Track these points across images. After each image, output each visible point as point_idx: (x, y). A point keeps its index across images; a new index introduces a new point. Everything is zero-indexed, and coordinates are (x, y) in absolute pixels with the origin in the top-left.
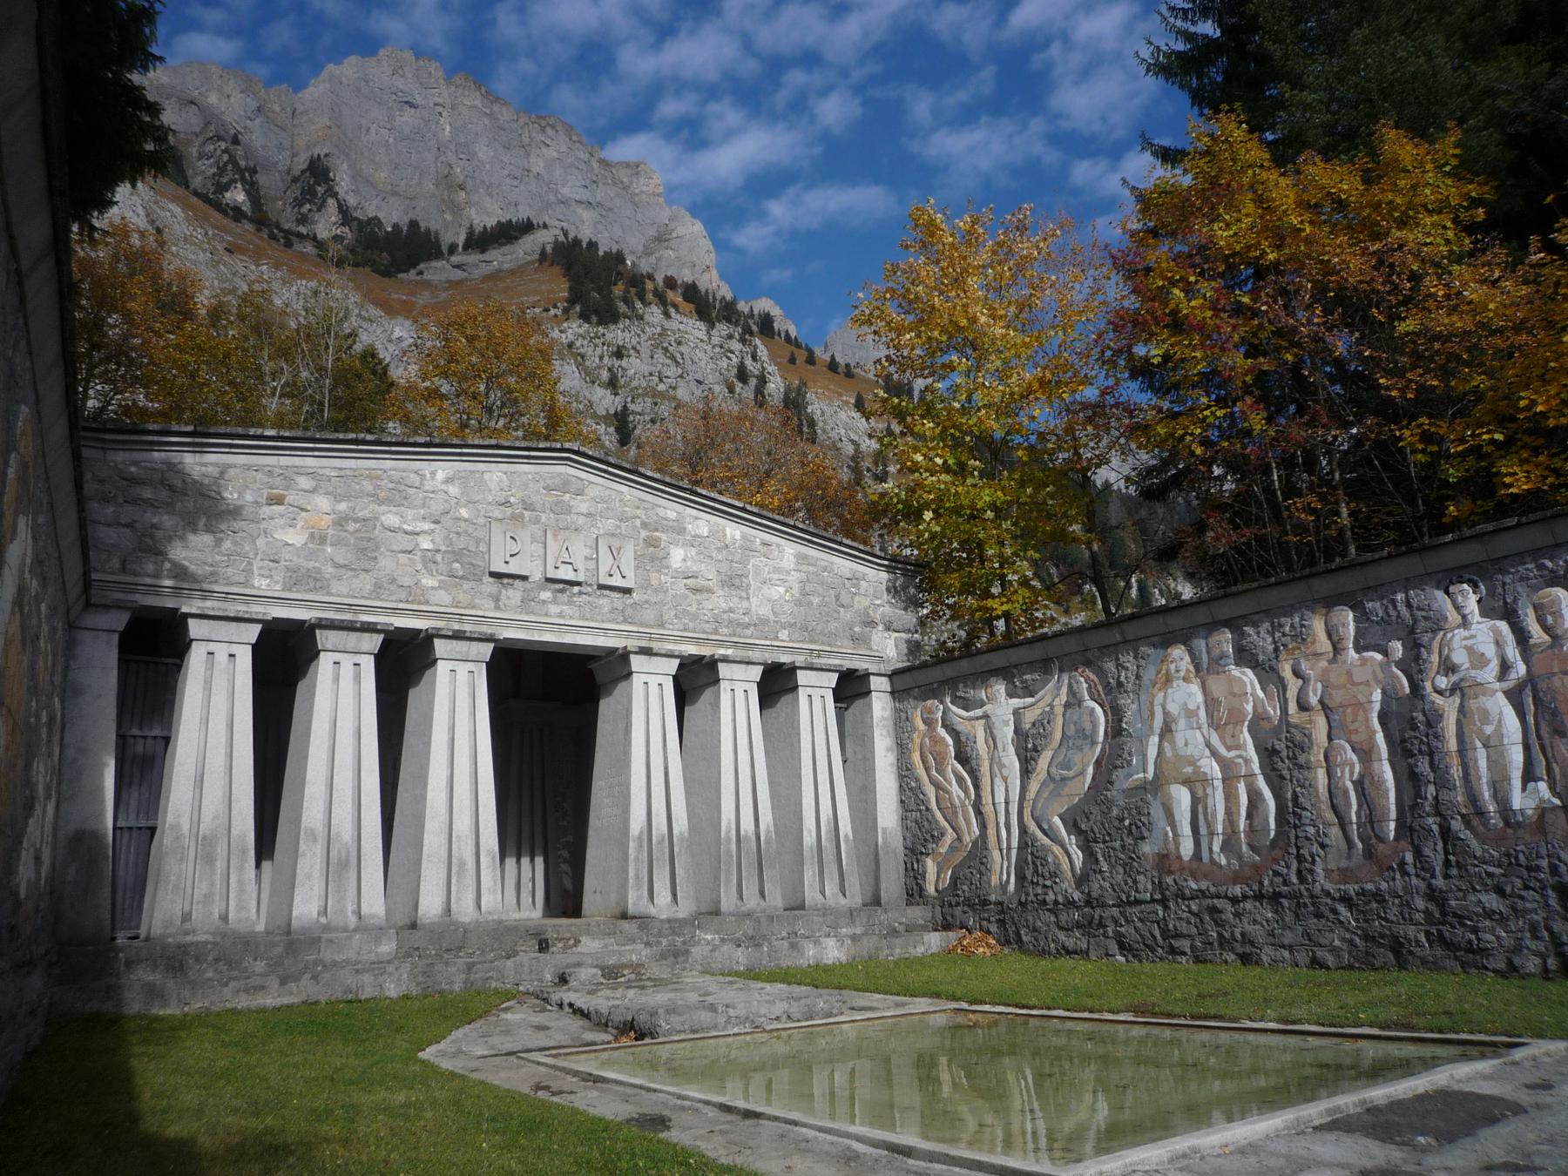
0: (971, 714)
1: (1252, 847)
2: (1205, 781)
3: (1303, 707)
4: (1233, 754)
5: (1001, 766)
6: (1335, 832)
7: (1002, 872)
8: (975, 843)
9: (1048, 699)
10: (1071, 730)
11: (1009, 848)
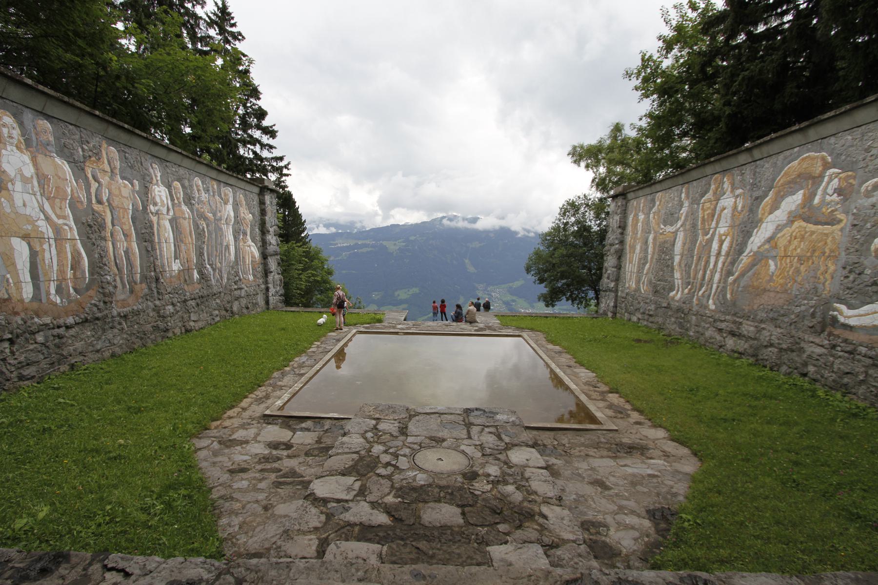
1: (75, 290)
2: (41, 238)
3: (100, 202)
4: (61, 222)
6: (118, 279)
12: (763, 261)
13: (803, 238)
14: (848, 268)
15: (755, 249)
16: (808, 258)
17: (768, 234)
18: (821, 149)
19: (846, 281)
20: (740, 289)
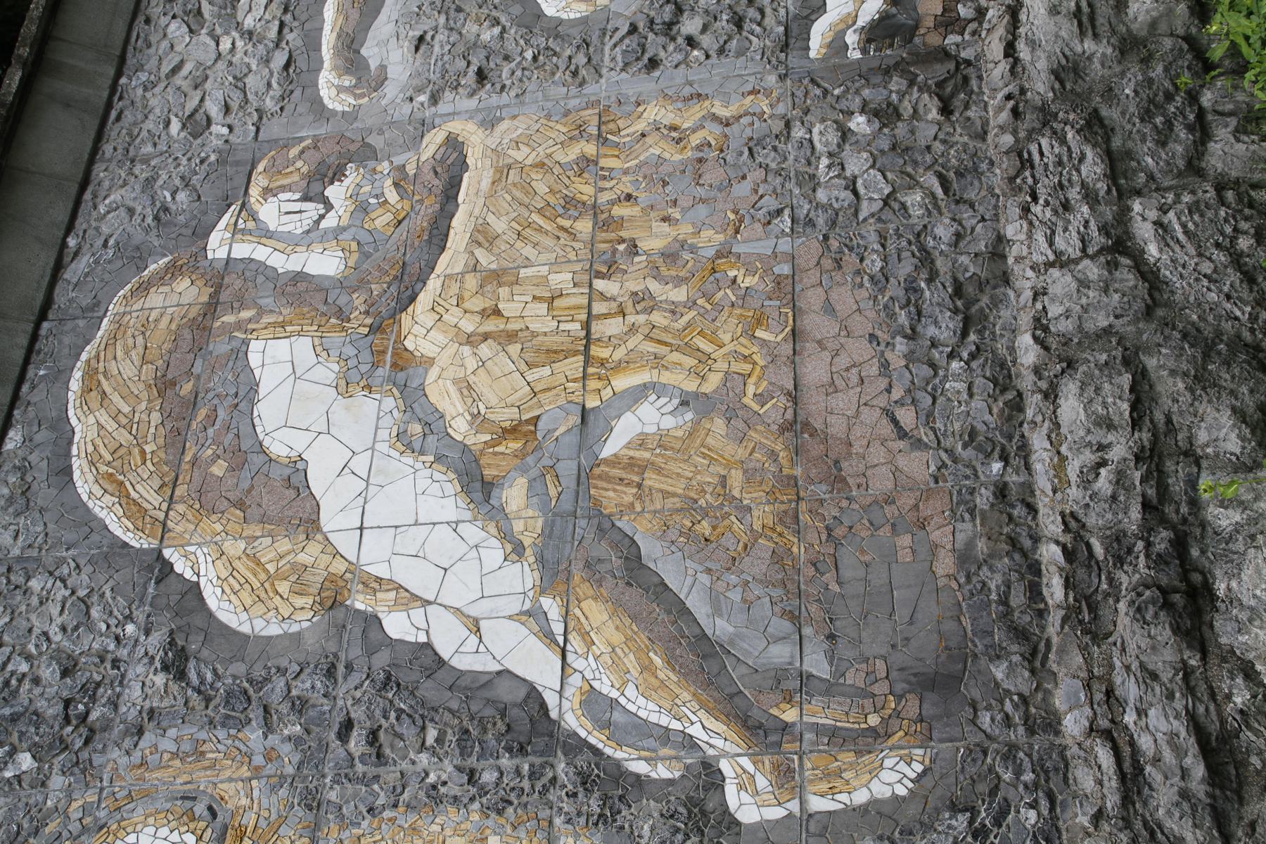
12: (611, 498)
13: (496, 277)
14: (654, 43)
15: (519, 578)
16: (604, 222)
17: (439, 498)
18: (94, 312)
19: (706, 40)
20: (817, 664)
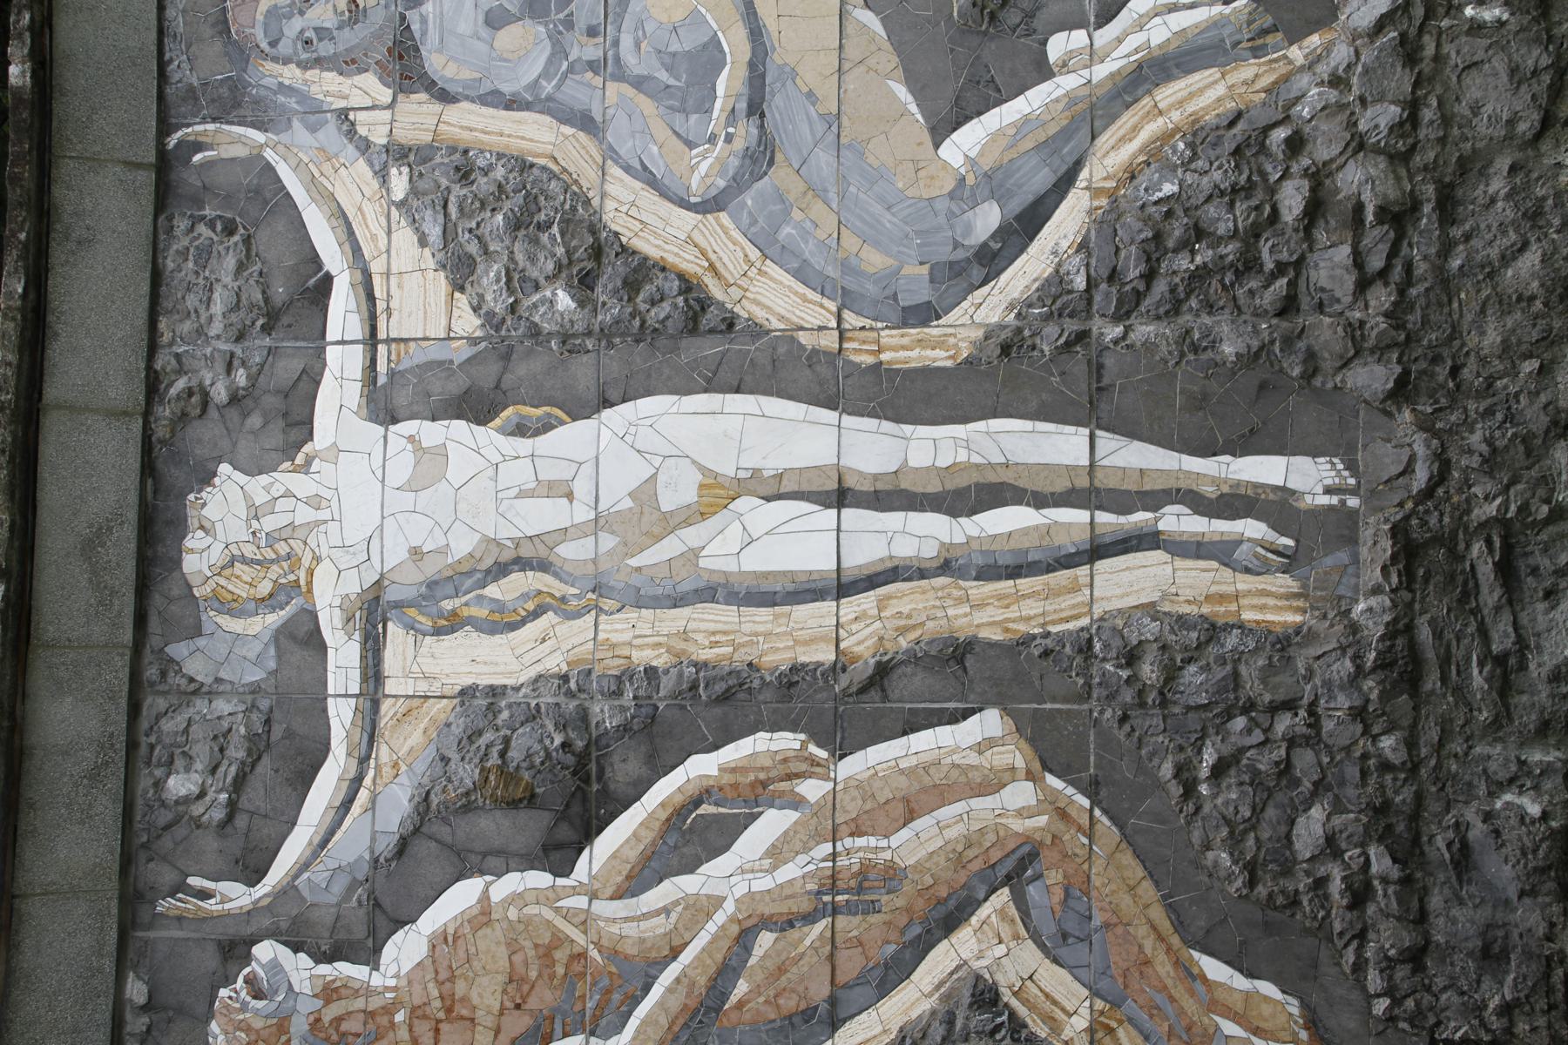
0: (341, 716)
5: (648, 517)
7: (1219, 543)
8: (1052, 750)
9: (354, 183)
10: (524, 51)
11: (1088, 494)
